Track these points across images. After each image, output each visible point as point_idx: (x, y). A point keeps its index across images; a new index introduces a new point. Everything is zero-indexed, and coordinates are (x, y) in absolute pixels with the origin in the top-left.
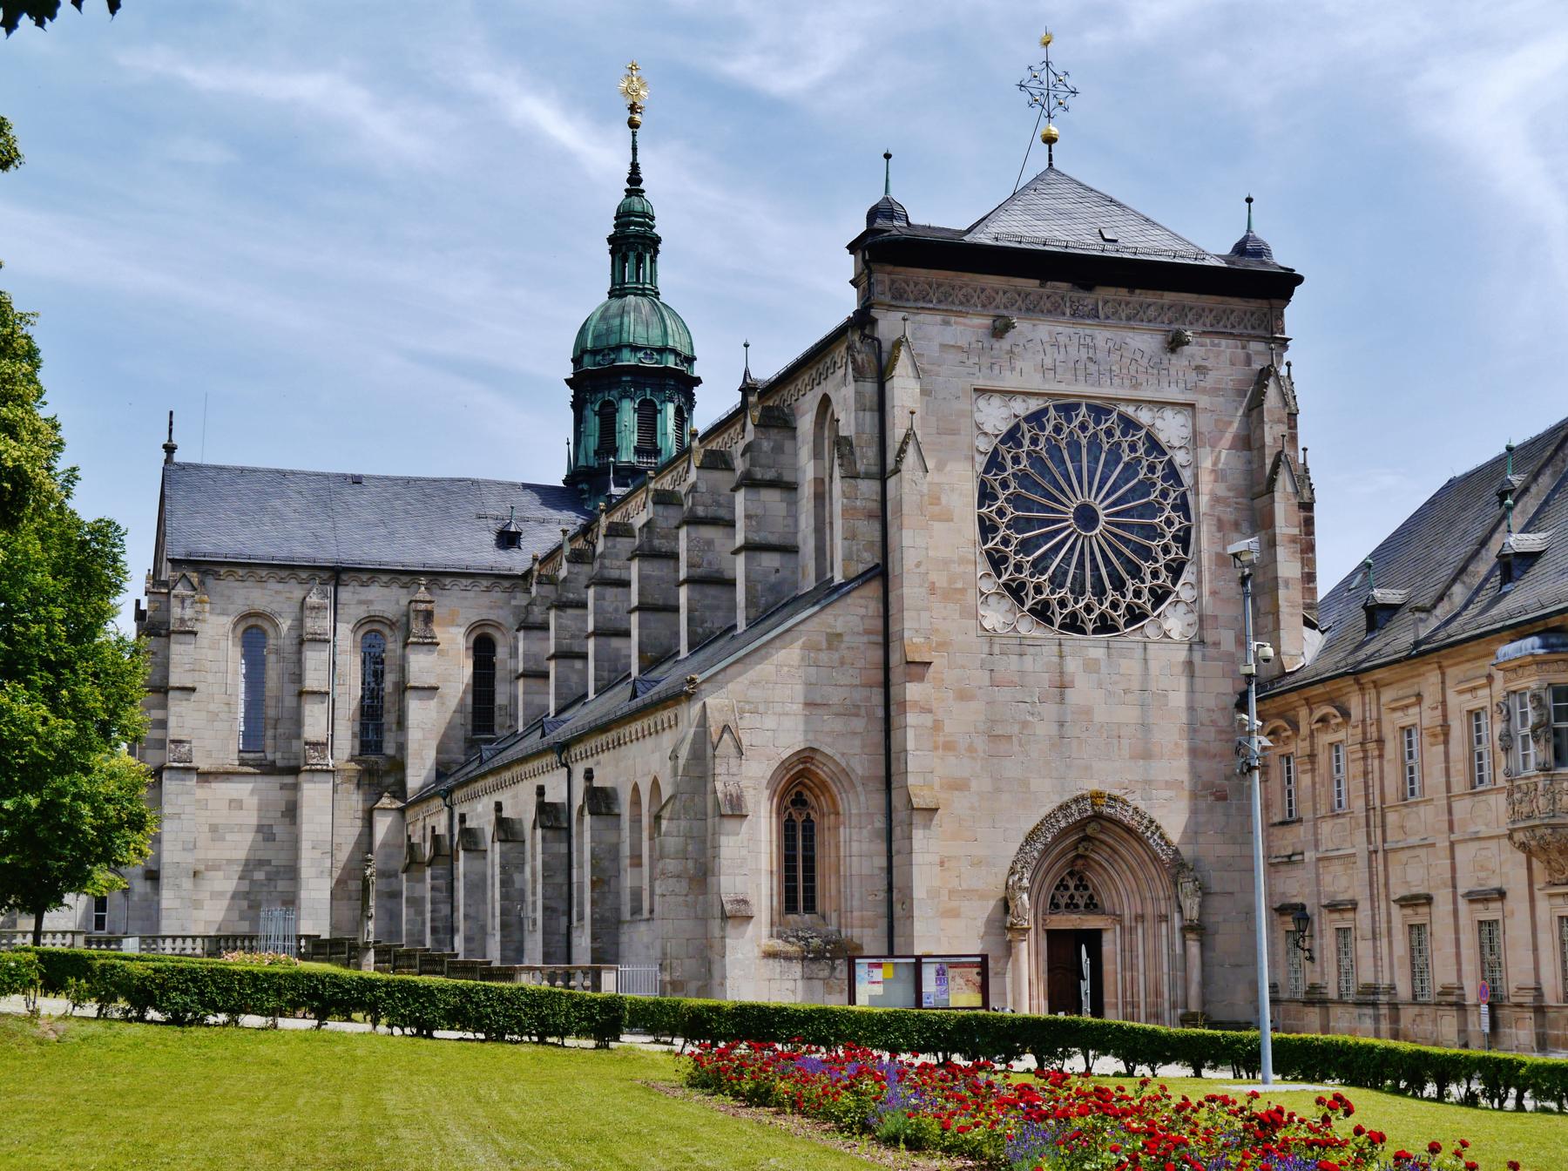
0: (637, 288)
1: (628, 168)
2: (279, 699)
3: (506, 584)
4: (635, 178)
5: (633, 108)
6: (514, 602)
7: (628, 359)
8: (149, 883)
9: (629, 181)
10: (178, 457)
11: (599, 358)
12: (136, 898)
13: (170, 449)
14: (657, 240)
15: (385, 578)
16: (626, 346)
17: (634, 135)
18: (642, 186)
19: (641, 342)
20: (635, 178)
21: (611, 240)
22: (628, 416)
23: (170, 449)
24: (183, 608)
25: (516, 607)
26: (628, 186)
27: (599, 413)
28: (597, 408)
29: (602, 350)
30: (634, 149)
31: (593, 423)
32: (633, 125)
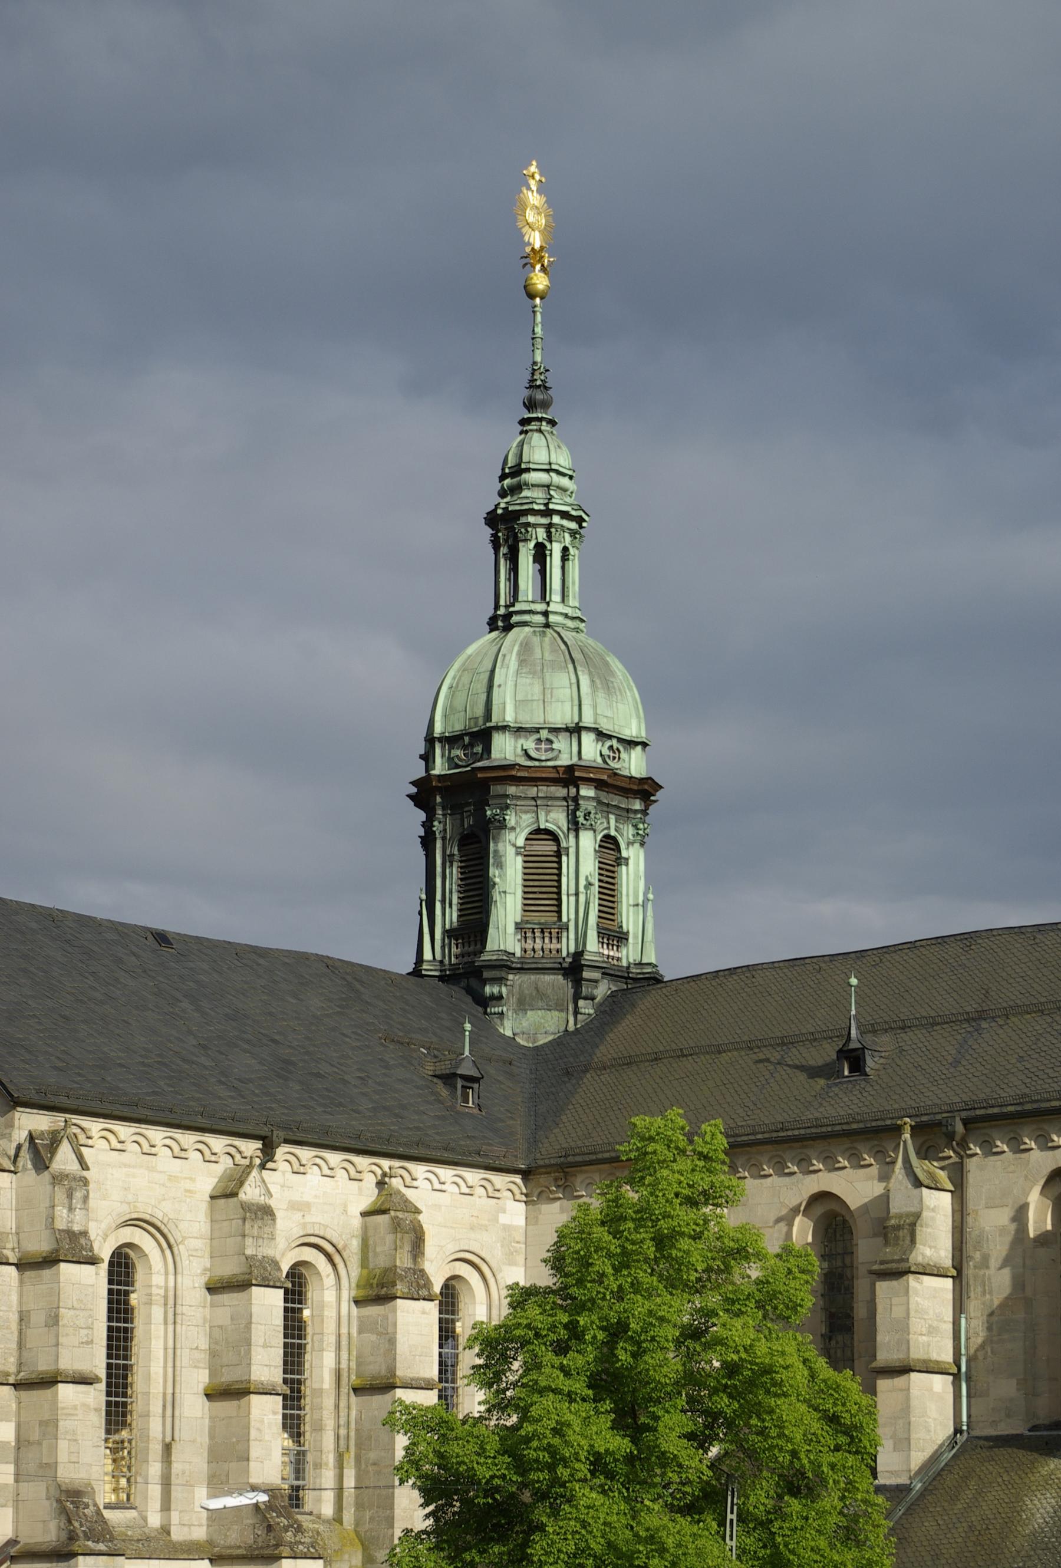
2: (171, 1403)
7: (591, 750)
11: (530, 744)
24: (71, 1209)
28: (521, 842)
29: (537, 730)
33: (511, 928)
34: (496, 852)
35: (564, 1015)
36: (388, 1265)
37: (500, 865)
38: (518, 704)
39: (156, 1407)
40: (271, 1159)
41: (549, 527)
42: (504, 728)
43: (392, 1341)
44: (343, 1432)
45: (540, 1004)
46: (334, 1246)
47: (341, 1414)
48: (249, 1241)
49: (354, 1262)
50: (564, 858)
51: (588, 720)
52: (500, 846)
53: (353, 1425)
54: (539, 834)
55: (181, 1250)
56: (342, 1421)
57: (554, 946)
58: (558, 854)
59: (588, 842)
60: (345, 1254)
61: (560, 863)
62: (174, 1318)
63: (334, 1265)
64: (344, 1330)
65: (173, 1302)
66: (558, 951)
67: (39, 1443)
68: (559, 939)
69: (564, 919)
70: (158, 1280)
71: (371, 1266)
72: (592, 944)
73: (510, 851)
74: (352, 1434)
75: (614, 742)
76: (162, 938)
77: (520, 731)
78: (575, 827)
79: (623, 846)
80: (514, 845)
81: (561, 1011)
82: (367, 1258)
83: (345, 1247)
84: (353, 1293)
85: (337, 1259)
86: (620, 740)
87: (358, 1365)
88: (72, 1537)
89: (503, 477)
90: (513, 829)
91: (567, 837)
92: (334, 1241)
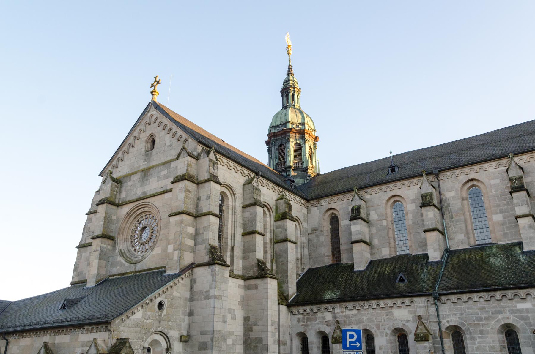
2: (234, 236)
6: (303, 211)
30: (289, 61)
32: (289, 54)
34: (288, 146)
35: (303, 180)
36: (284, 212)
39: (229, 237)
43: (286, 230)
44: (272, 254)
45: (298, 177)
46: (270, 206)
47: (272, 249)
48: (255, 195)
49: (274, 211)
50: (302, 149)
52: (289, 145)
53: (275, 252)
54: (297, 144)
55: (237, 196)
56: (272, 251)
57: (301, 166)
58: (301, 148)
60: (272, 209)
61: (301, 150)
62: (234, 213)
63: (269, 212)
64: (272, 228)
65: (234, 209)
67: (203, 233)
69: (303, 160)
70: (230, 203)
71: (279, 212)
74: (275, 254)
81: (303, 179)
82: (278, 211)
83: (272, 207)
84: (274, 219)
85: (270, 210)
87: (276, 237)
88: (213, 259)
89: (284, 83)
91: (303, 145)
92: (270, 205)
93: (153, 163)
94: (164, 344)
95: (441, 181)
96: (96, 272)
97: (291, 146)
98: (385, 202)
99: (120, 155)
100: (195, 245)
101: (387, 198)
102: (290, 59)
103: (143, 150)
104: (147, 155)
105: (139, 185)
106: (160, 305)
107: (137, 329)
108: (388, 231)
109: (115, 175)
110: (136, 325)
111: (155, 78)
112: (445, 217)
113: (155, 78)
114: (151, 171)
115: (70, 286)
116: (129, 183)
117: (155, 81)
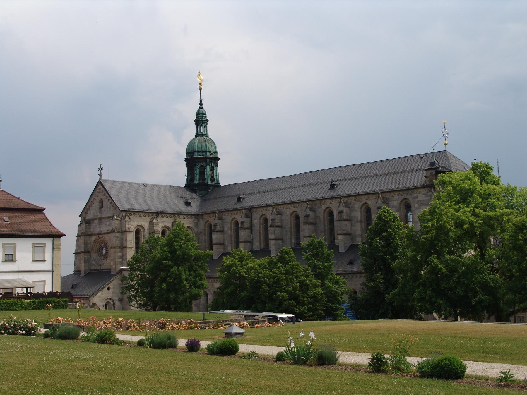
0: (205, 135)
1: (199, 101)
3: (193, 217)
4: (201, 104)
5: (200, 84)
6: (194, 222)
7: (209, 155)
8: (119, 302)
9: (200, 104)
10: (103, 178)
11: (199, 153)
12: (117, 307)
13: (100, 175)
14: (207, 121)
15: (168, 215)
16: (208, 151)
17: (200, 91)
18: (203, 106)
19: (211, 150)
20: (201, 104)
21: (195, 121)
22: (208, 169)
23: (100, 175)
24: (128, 225)
25: (195, 223)
26: (199, 106)
27: (199, 169)
28: (199, 167)
29: (200, 152)
30: (201, 95)
31: (197, 172)
32: (200, 89)
33: (198, 180)
37: (196, 171)
38: (198, 148)
40: (158, 216)
41: (202, 122)
42: (196, 151)
51: (208, 150)
54: (201, 166)
57: (204, 182)
59: (208, 167)
66: (205, 182)
68: (205, 181)
69: (205, 178)
70: (142, 233)
72: (209, 182)
73: (197, 169)
75: (212, 153)
76: (145, 185)
77: (198, 152)
78: (207, 165)
79: (214, 167)
80: (198, 168)
86: (213, 152)
90: (198, 166)
93: (103, 216)
94: (112, 302)
95: (253, 214)
96: (84, 269)
97: (197, 169)
98: (230, 221)
99: (88, 207)
100: (122, 261)
101: (231, 219)
102: (202, 94)
103: (98, 207)
104: (100, 210)
105: (98, 226)
106: (109, 289)
107: (99, 299)
108: (231, 237)
109: (87, 218)
110: (99, 297)
111: (100, 165)
112: (253, 233)
113: (100, 165)
114: (103, 220)
115: (74, 273)
116: (94, 225)
117: (100, 168)
